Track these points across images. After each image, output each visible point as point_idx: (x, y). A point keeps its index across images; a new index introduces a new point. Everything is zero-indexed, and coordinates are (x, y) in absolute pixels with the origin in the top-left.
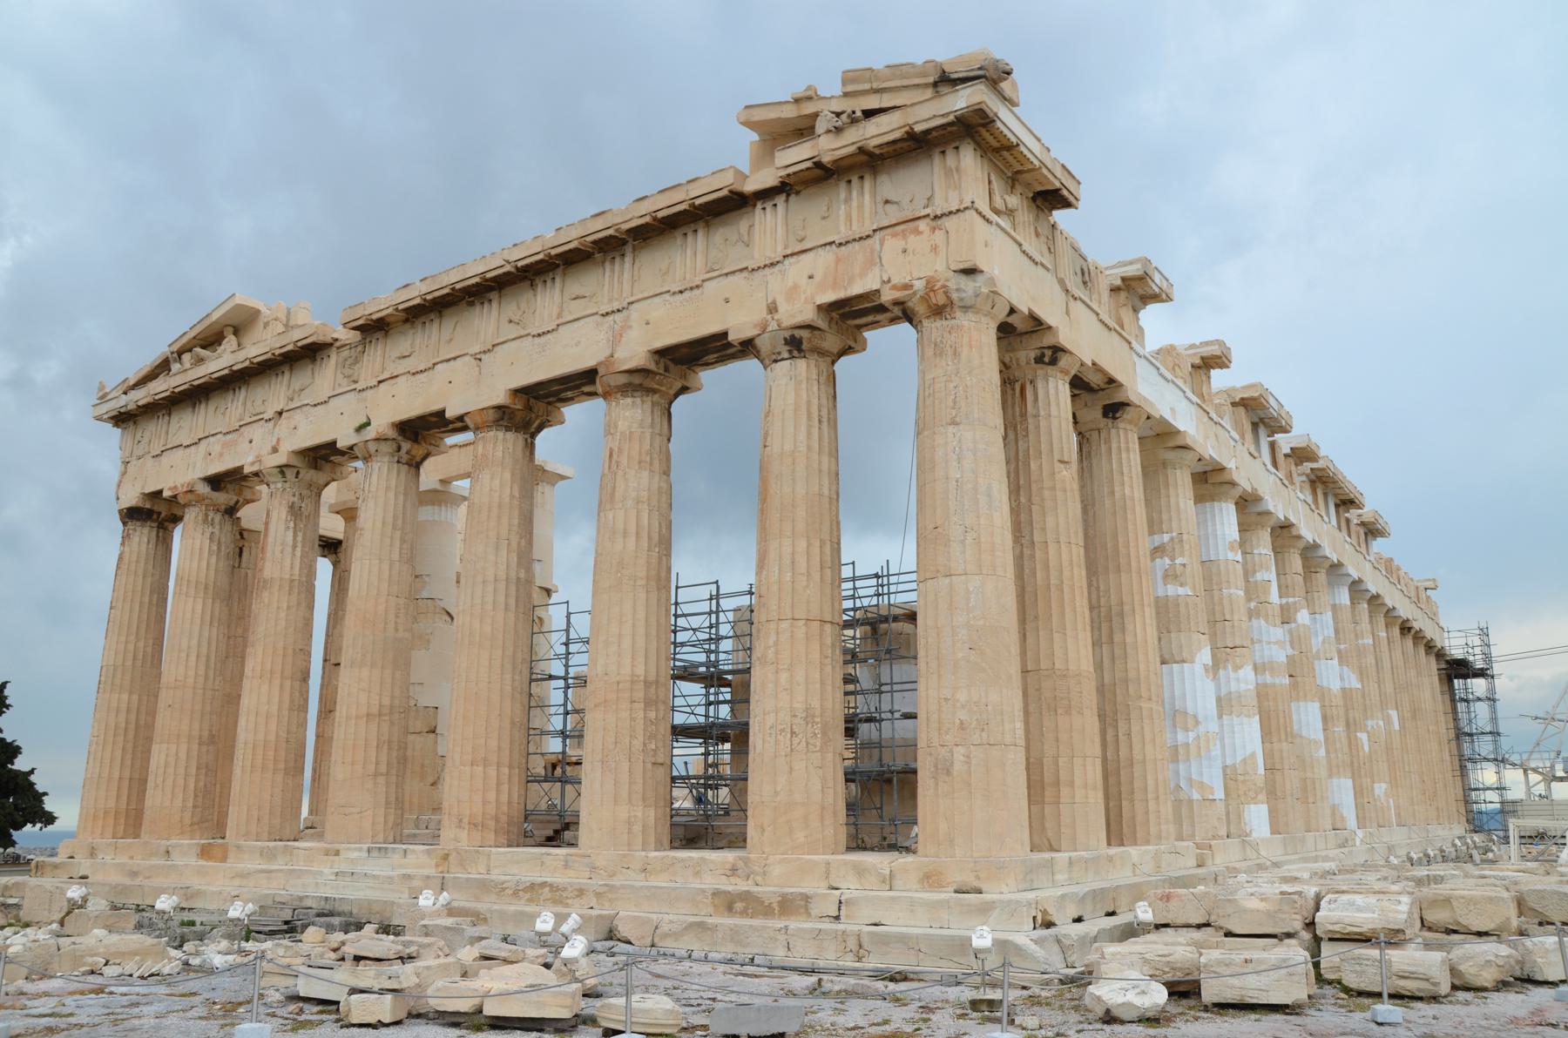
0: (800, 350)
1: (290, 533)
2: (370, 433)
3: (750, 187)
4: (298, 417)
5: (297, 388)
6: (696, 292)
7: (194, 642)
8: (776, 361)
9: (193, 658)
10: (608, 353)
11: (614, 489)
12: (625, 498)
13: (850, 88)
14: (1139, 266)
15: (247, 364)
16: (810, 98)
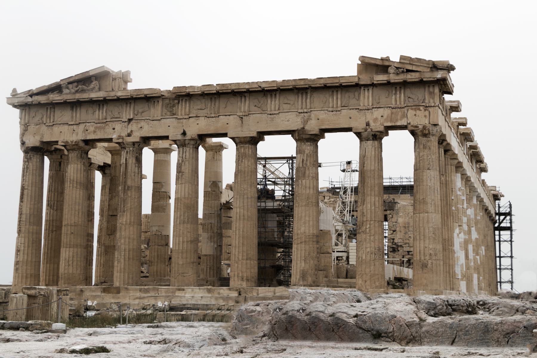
0: (376, 138)
1: (137, 168)
2: (188, 137)
3: (362, 83)
4: (142, 124)
5: (140, 111)
6: (338, 112)
7: (80, 207)
8: (367, 140)
9: (80, 214)
10: (302, 126)
11: (305, 172)
12: (309, 177)
13: (402, 61)
14: (457, 103)
15: (116, 98)
16: (387, 60)
